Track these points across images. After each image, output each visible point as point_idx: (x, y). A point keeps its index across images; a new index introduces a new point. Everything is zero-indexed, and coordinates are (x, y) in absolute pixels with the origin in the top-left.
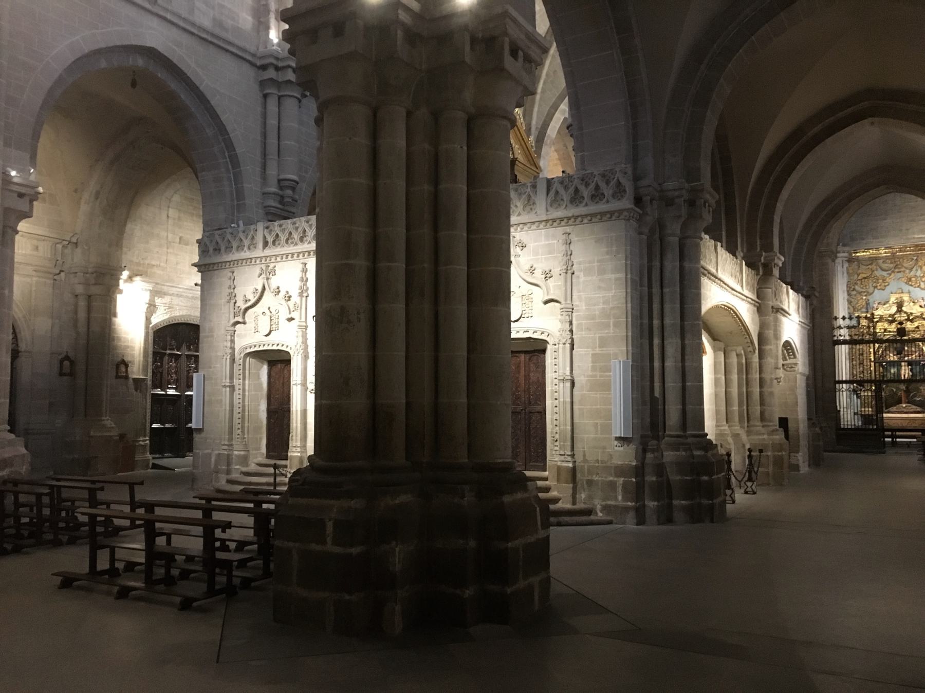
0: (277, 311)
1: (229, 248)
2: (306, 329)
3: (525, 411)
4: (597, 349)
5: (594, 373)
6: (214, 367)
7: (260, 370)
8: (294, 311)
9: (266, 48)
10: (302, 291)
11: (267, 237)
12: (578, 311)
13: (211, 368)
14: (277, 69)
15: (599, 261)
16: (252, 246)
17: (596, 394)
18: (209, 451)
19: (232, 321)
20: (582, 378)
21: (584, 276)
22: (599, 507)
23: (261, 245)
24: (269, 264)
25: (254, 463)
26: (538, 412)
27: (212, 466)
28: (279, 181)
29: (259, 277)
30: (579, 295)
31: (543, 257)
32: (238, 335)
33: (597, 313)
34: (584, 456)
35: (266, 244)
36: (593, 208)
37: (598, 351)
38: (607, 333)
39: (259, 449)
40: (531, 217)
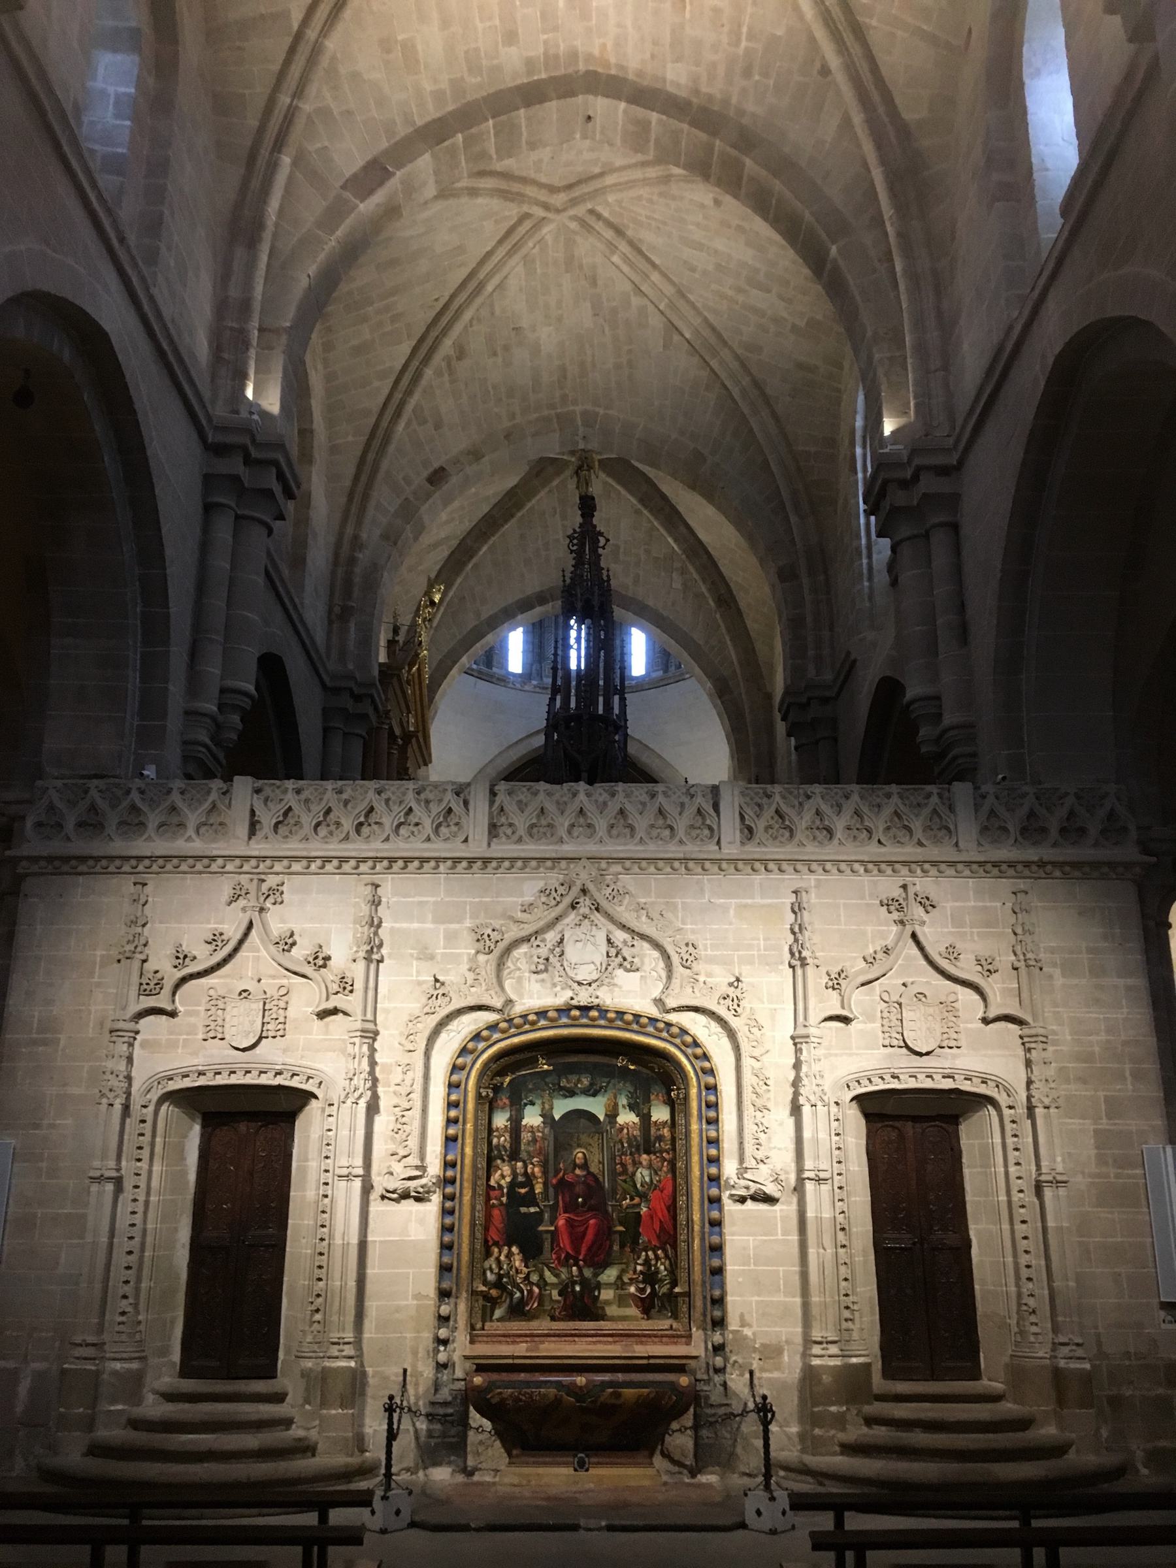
1: (134, 824)
2: (374, 1040)
4: (1104, 1121)
5: (1104, 1170)
6: (52, 1126)
8: (337, 993)
9: (237, 412)
10: (372, 948)
11: (257, 813)
13: (37, 1126)
14: (248, 461)
15: (1090, 950)
16: (213, 825)
17: (1112, 1213)
18: (11, 1364)
19: (134, 1008)
20: (1079, 1178)
21: (1064, 976)
22: (1140, 1454)
23: (243, 830)
24: (263, 877)
25: (155, 1392)
27: (19, 1409)
28: (223, 691)
29: (230, 903)
32: (144, 1045)
33: (1097, 1049)
34: (1099, 1344)
35: (253, 827)
36: (1069, 853)
37: (1104, 1124)
39: (165, 1351)
40: (943, 851)
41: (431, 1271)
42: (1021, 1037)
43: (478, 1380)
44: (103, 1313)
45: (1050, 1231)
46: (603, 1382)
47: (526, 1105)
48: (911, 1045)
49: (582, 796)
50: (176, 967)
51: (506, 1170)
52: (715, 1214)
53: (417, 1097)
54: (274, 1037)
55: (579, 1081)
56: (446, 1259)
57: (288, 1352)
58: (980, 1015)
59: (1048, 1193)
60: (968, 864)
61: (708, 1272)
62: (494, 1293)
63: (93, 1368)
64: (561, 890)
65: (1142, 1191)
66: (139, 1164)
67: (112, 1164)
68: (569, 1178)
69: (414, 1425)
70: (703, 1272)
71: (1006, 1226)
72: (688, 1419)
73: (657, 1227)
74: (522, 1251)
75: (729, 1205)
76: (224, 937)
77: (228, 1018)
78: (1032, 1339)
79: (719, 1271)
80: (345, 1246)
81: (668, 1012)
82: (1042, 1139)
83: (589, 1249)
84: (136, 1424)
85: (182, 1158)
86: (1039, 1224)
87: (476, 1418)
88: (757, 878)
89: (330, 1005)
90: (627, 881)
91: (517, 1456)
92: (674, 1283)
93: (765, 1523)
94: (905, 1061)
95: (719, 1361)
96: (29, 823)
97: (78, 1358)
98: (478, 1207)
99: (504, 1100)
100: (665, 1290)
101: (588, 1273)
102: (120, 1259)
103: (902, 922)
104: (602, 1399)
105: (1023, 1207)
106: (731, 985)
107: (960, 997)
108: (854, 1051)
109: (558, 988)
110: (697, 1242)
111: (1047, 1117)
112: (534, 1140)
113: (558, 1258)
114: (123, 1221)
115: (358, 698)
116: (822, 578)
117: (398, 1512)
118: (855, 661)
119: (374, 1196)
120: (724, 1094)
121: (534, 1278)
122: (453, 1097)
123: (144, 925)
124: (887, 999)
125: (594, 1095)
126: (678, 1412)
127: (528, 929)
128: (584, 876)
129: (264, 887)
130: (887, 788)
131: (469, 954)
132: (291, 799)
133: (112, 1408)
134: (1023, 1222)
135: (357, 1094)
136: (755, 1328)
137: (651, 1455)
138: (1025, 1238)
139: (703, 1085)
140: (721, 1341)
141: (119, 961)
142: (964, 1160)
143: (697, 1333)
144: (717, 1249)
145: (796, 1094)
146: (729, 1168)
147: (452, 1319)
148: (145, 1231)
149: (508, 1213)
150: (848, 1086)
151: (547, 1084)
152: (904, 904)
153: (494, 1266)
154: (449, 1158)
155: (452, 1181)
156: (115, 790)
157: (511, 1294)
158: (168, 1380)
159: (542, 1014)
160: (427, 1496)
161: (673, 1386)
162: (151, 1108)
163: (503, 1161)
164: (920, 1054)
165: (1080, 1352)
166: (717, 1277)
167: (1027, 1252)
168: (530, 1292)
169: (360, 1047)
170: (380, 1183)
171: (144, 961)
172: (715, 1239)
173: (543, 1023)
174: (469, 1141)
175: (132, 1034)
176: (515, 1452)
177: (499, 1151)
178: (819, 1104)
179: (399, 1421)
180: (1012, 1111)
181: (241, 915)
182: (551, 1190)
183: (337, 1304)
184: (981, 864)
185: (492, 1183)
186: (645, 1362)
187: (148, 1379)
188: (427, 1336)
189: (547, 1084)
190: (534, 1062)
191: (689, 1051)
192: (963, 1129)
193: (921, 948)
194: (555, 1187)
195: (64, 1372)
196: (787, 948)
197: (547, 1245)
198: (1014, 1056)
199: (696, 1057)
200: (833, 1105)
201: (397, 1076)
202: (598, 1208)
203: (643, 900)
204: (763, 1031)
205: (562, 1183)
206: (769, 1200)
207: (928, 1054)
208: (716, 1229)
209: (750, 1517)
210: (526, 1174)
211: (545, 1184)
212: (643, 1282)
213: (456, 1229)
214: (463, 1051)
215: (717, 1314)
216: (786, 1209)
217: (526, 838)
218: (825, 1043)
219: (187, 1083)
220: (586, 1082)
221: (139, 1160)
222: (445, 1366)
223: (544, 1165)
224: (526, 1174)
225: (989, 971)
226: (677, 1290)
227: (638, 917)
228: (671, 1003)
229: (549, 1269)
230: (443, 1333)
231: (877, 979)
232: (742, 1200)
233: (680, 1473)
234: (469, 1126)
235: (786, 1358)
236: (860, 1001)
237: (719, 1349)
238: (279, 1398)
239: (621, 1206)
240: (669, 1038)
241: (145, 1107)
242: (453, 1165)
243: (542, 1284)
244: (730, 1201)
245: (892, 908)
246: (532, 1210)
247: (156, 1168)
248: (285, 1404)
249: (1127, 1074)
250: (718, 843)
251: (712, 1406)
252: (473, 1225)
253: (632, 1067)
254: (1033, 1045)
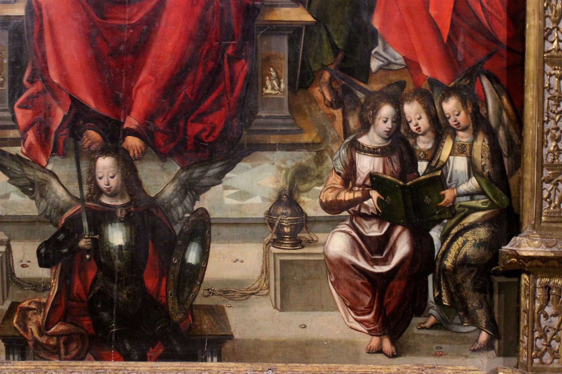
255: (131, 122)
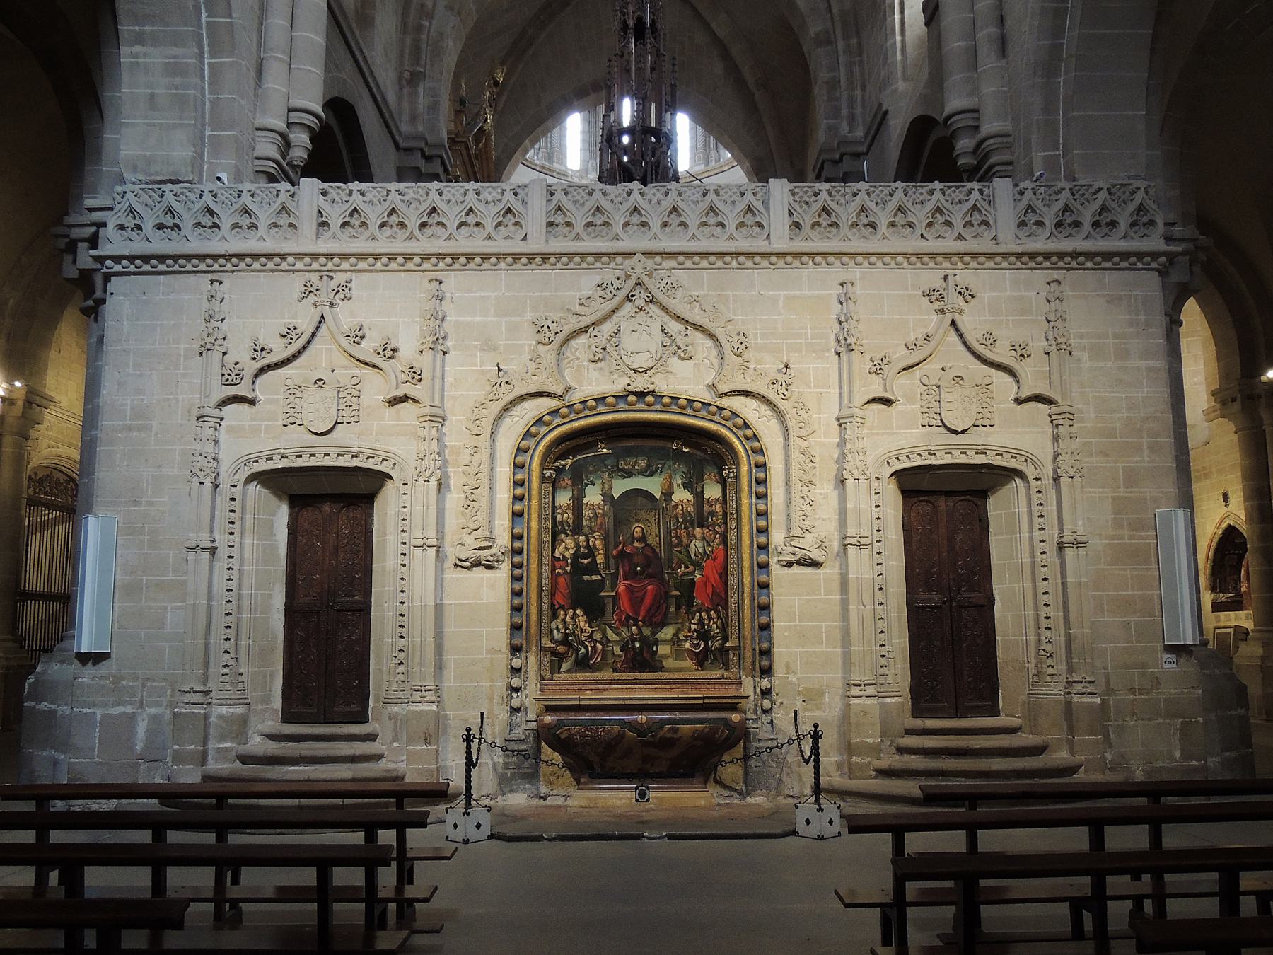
0: (355, 381)
3: (951, 603)
6: (150, 504)
7: (274, 516)
12: (1082, 420)
13: (136, 503)
15: (1116, 336)
17: (1125, 570)
18: (129, 709)
21: (1091, 360)
26: (977, 606)
30: (1081, 393)
31: (1010, 318)
32: (231, 430)
34: (1108, 682)
37: (1122, 492)
38: (1137, 462)
39: (266, 700)
41: (503, 629)
42: (1050, 416)
43: (548, 719)
44: (206, 665)
45: (1069, 585)
46: (661, 719)
47: (587, 485)
48: (947, 424)
49: (636, 194)
50: (254, 359)
51: (570, 543)
52: (763, 578)
53: (484, 476)
54: (348, 423)
55: (636, 463)
56: (517, 620)
57: (377, 700)
58: (1013, 396)
59: (1069, 552)
60: (1006, 255)
61: (757, 627)
62: (561, 649)
63: (202, 712)
64: (617, 284)
65: (1153, 552)
66: (231, 537)
67: (207, 536)
68: (628, 550)
69: (492, 760)
70: (753, 628)
71: (1028, 584)
72: (738, 751)
73: (710, 591)
74: (585, 613)
75: (776, 569)
76: (298, 331)
77: (305, 405)
78: (1048, 679)
79: (766, 627)
80: (423, 607)
81: (720, 396)
82: (1065, 505)
83: (648, 611)
84: (244, 759)
85: (272, 534)
86: (1059, 581)
87: (548, 752)
88: (805, 272)
89: (400, 393)
90: (680, 275)
91: (585, 783)
92: (726, 639)
93: (813, 830)
94: (942, 439)
95: (766, 703)
96: (111, 226)
97: (187, 703)
98: (545, 575)
99: (566, 480)
100: (717, 645)
101: (647, 632)
102: (219, 620)
103: (943, 311)
104: (662, 733)
105: (1045, 566)
106: (779, 371)
107: (995, 380)
108: (895, 431)
109: (616, 376)
110: (747, 602)
111: (1072, 486)
112: (596, 517)
113: (620, 620)
114: (220, 586)
115: (428, 158)
116: (854, 41)
117: (478, 826)
118: (886, 113)
119: (449, 563)
120: (772, 472)
121: (598, 636)
122: (519, 477)
123: (222, 320)
124: (927, 383)
125: (651, 476)
126: (729, 744)
127: (585, 321)
128: (639, 270)
129: (334, 284)
130: (930, 186)
131: (530, 345)
132: (357, 199)
133: (221, 746)
134: (1045, 579)
135: (427, 474)
136: (799, 675)
137: (706, 782)
138: (1046, 593)
139: (752, 463)
140: (769, 687)
141: (201, 354)
142: (990, 530)
143: (747, 682)
144: (765, 608)
145: (841, 470)
146: (777, 537)
147: (523, 671)
148: (240, 597)
149: (572, 579)
150: (888, 463)
151: (606, 466)
152: (944, 294)
153: (560, 627)
154: (516, 531)
155: (519, 552)
156: (188, 194)
157: (577, 651)
158: (273, 724)
159: (600, 400)
160: (504, 816)
161: (726, 722)
162: (240, 487)
163: (567, 535)
164: (956, 432)
165: (1091, 688)
166: (765, 633)
167: (1046, 605)
168: (594, 648)
169: (430, 430)
170: (452, 552)
171: (224, 354)
172: (764, 600)
173: (601, 408)
174: (534, 516)
175: (218, 420)
176: (583, 780)
177: (563, 526)
178: (862, 477)
179: (478, 755)
180: (1039, 482)
181: (313, 310)
182: (612, 561)
183: (417, 660)
184: (1019, 255)
185: (557, 554)
186: (700, 702)
187: (253, 721)
188: (501, 685)
189: (606, 466)
190: (592, 446)
191: (740, 433)
192: (991, 502)
193: (961, 336)
194: (614, 557)
195: (175, 715)
196: (833, 337)
197: (609, 608)
198: (1043, 432)
199: (747, 438)
200: (873, 478)
201: (465, 458)
202: (657, 577)
203: (697, 293)
204: (810, 413)
205: (622, 555)
206: (814, 564)
207: (963, 432)
208: (765, 591)
209: (800, 826)
210: (588, 546)
211: (606, 556)
212: (697, 639)
213: (524, 593)
214: (527, 435)
215: (765, 663)
216: (830, 571)
217: (584, 236)
218: (868, 424)
219: (270, 465)
220: (642, 463)
221: (232, 534)
222: (518, 710)
223: (605, 539)
224: (588, 546)
225: (1022, 355)
226: (728, 645)
227: (692, 308)
228: (724, 388)
229: (611, 628)
230: (516, 682)
231: (918, 364)
232: (789, 564)
233: (732, 796)
234: (534, 503)
235: (827, 699)
236: (901, 386)
237: (766, 693)
238: (372, 737)
239: (676, 573)
240: (721, 421)
241: (233, 486)
242: (520, 537)
243: (605, 641)
244: (778, 566)
245: (933, 298)
246: (594, 578)
247: (248, 541)
248: (376, 743)
249: (1145, 447)
250: (768, 237)
251: (759, 740)
252: (540, 592)
253: (687, 450)
254: (1060, 422)
255: (640, 619)
